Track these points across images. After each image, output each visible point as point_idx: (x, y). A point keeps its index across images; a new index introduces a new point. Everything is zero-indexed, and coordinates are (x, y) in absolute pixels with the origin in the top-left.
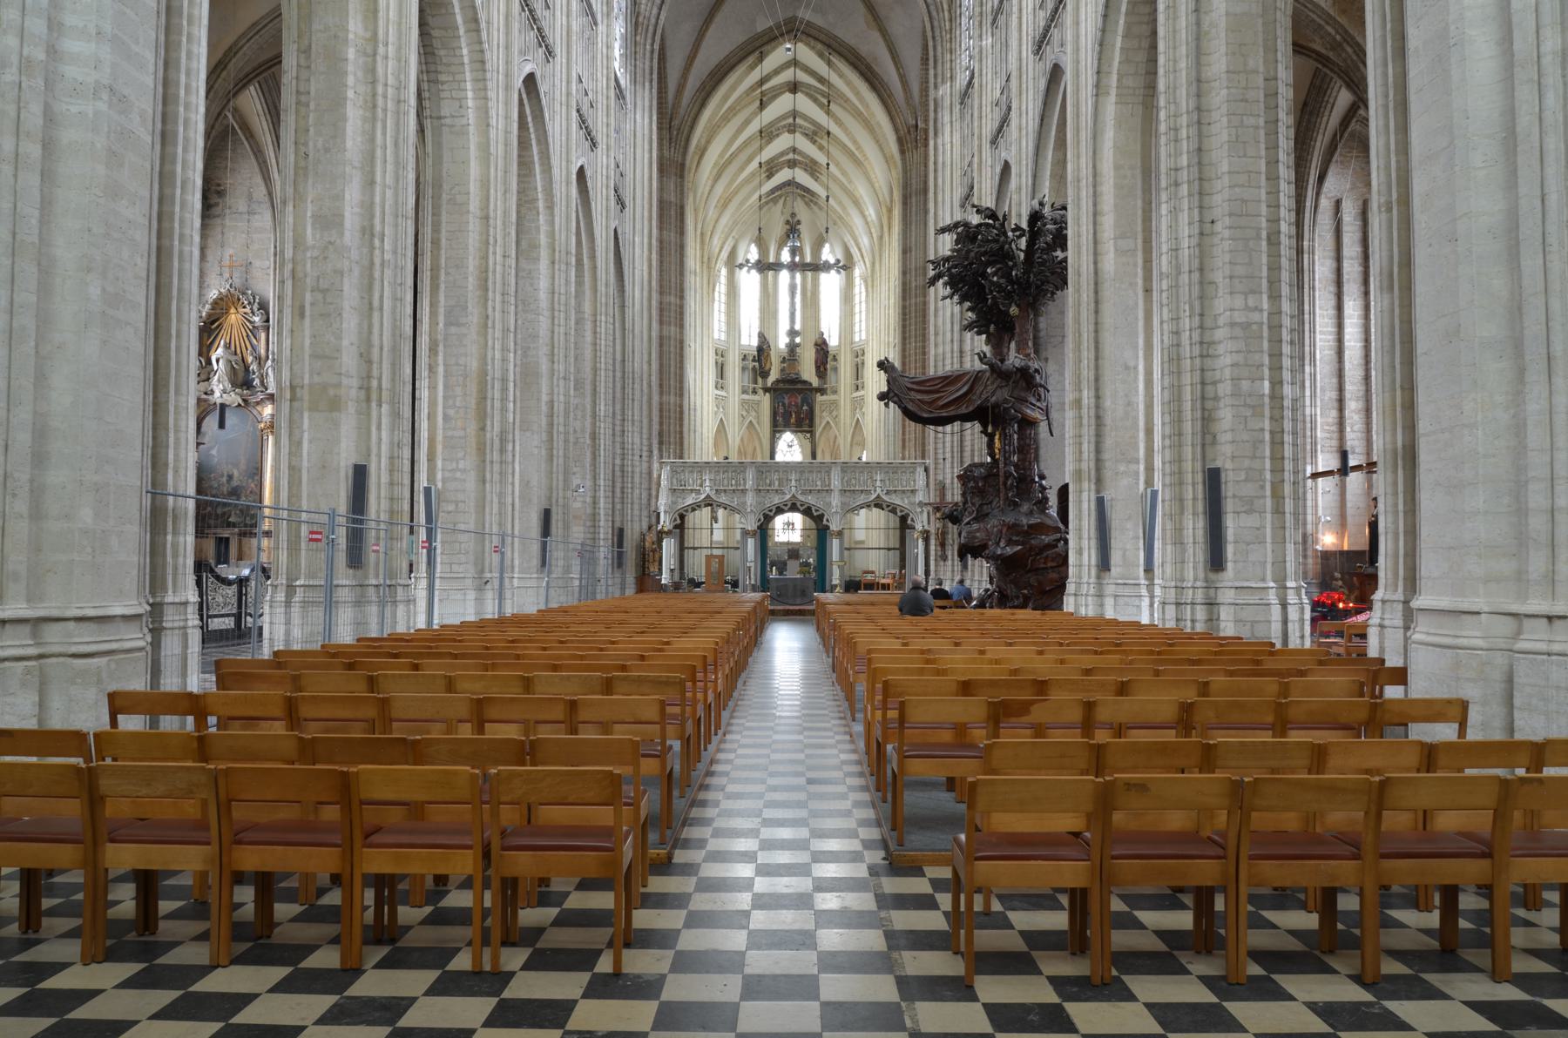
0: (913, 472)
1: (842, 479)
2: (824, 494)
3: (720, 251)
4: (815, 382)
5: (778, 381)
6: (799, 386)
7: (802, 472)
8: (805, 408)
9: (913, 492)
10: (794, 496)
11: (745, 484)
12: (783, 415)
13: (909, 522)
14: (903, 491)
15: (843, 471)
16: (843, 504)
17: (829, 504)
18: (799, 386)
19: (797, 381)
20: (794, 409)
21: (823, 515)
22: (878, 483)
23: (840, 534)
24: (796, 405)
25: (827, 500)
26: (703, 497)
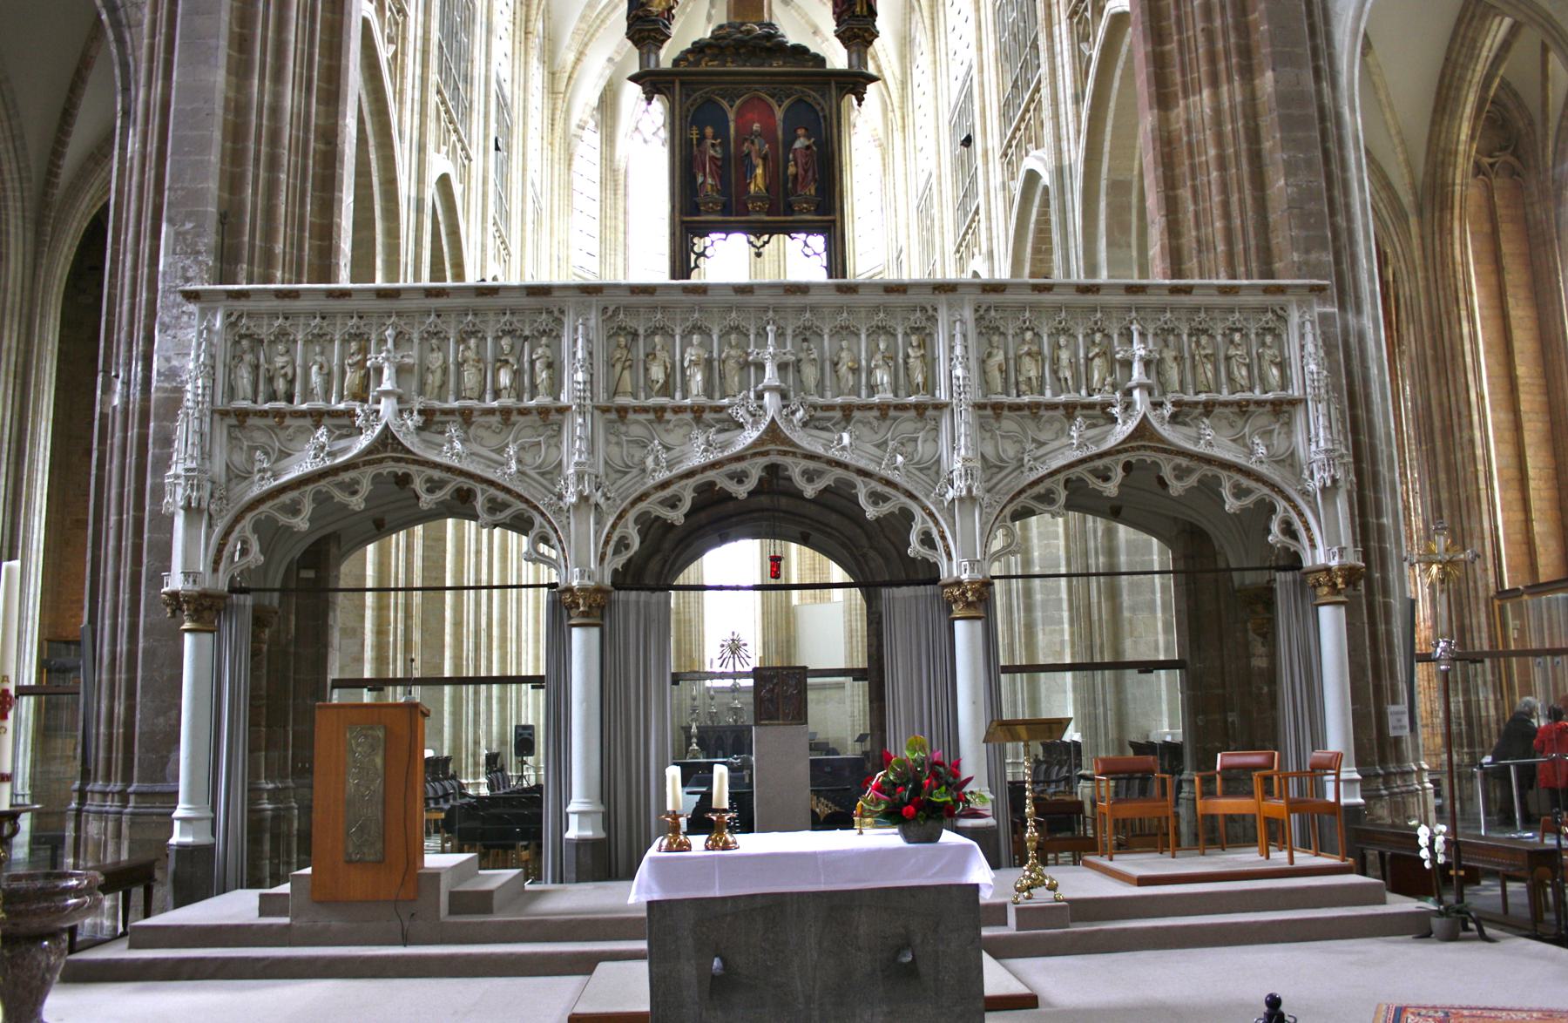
0: (1274, 333)
1: (983, 362)
2: (907, 424)
3: (578, 60)
4: (837, 57)
5: (699, 48)
6: (777, 66)
7: (806, 334)
8: (800, 143)
9: (1283, 409)
10: (773, 431)
11: (555, 387)
12: (722, 168)
13: (1275, 536)
14: (1243, 409)
15: (987, 328)
16: (991, 467)
17: (933, 468)
18: (777, 66)
19: (771, 45)
20: (757, 147)
21: (906, 517)
22: (1137, 372)
23: (980, 599)
24: (768, 134)
25: (923, 449)
26: (363, 442)
